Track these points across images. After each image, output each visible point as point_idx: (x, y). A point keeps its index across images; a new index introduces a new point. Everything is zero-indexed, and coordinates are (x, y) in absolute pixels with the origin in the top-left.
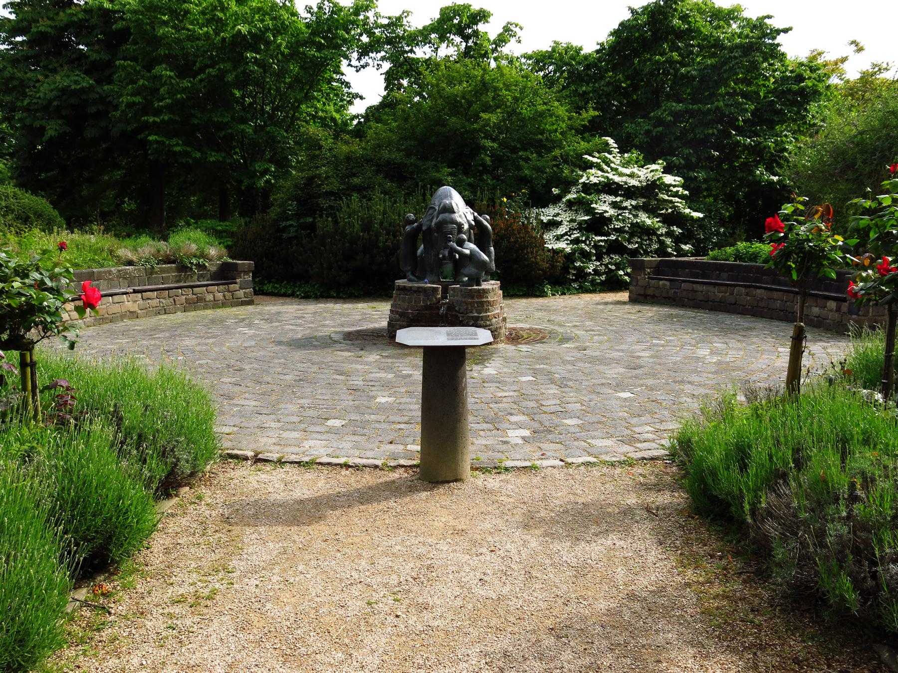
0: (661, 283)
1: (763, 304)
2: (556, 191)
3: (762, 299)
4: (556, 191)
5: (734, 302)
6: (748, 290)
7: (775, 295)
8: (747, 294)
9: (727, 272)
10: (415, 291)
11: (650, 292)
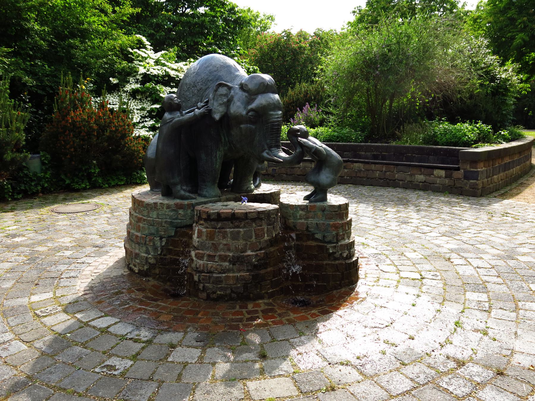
1: (362, 175)
2: (114, 81)
3: (360, 171)
4: (114, 81)
7: (373, 167)
10: (254, 220)
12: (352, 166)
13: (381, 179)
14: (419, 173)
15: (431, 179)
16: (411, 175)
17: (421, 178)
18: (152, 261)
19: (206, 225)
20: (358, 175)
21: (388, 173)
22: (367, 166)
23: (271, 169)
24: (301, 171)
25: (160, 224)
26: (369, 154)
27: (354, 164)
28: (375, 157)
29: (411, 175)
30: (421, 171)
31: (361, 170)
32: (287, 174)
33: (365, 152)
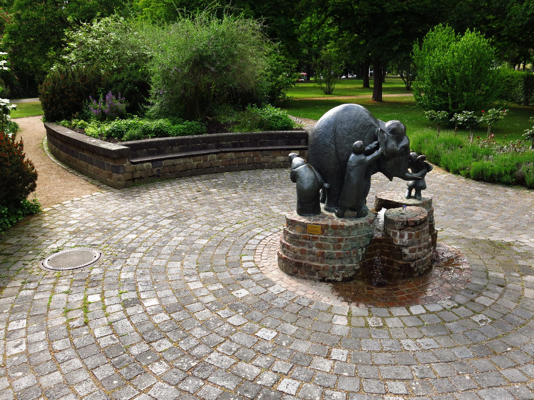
0: (145, 165)
1: (234, 162)
3: (232, 159)
5: (209, 166)
6: (219, 155)
7: (242, 154)
8: (220, 158)
9: (178, 146)
11: (137, 175)
12: (225, 156)
13: (250, 164)
16: (274, 157)
18: (357, 268)
19: (413, 229)
21: (255, 158)
22: (238, 155)
23: (155, 170)
24: (183, 167)
25: (360, 238)
27: (227, 154)
28: (235, 145)
29: (274, 157)
30: (281, 153)
32: (170, 172)
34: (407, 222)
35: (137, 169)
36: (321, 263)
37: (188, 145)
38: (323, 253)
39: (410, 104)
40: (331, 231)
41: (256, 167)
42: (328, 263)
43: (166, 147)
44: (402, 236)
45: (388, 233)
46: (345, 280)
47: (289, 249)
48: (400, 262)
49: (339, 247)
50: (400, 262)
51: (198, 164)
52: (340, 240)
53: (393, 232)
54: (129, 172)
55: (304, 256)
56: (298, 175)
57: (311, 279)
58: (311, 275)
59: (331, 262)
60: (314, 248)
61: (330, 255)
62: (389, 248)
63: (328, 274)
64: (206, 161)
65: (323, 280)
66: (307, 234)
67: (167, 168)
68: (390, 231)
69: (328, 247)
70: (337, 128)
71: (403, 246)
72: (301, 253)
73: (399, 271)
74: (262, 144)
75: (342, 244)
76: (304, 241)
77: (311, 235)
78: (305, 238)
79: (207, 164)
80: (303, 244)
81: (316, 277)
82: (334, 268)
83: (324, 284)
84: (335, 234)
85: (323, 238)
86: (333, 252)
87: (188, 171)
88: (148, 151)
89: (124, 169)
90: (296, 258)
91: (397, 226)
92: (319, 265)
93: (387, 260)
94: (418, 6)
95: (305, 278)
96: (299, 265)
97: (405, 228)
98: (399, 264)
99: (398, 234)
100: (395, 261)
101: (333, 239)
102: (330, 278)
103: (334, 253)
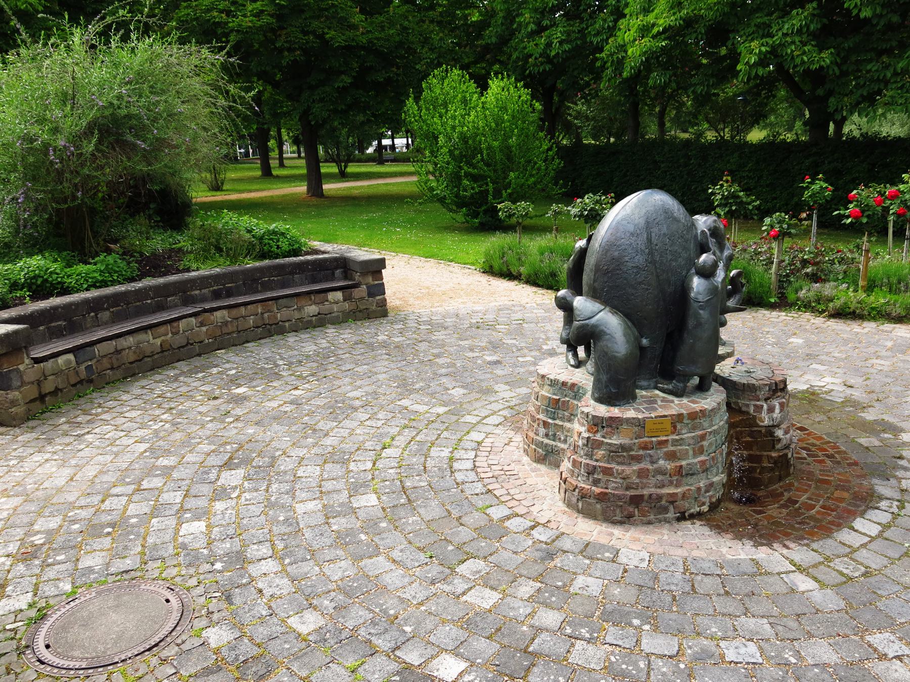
1: (231, 328)
3: (225, 323)
5: (184, 342)
8: (202, 324)
9: (107, 309)
11: (48, 387)
12: (212, 317)
14: (310, 303)
15: (326, 307)
16: (299, 309)
17: (312, 309)
20: (225, 330)
22: (235, 312)
23: (83, 367)
24: (135, 352)
26: (205, 291)
27: (215, 313)
28: (217, 295)
30: (311, 299)
31: (228, 322)
32: (112, 369)
33: (200, 290)
34: (776, 383)
35: (47, 373)
36: (677, 486)
37: (128, 305)
38: (681, 467)
39: (413, 197)
40: (688, 424)
41: (269, 331)
42: (687, 485)
43: (84, 315)
44: (771, 410)
45: (744, 409)
46: (714, 507)
47: (612, 475)
48: (774, 454)
49: (701, 451)
50: (774, 454)
51: (163, 341)
52: (703, 437)
53: (755, 405)
54: (32, 383)
55: (645, 481)
56: (602, 331)
57: (660, 521)
58: (660, 514)
59: (690, 480)
60: (661, 462)
61: (691, 469)
62: (751, 434)
63: (689, 503)
64: (177, 333)
65: (682, 517)
66: (646, 439)
67: (105, 360)
68: (748, 406)
69: (685, 455)
70: (653, 235)
71: (774, 426)
72: (639, 477)
73: (772, 470)
74: (267, 287)
75: (705, 443)
76: (641, 452)
77: (654, 439)
78: (645, 448)
79: (180, 340)
80: (638, 459)
81: (671, 515)
82: (699, 489)
83: (688, 524)
84: (694, 428)
85: (677, 440)
86: (696, 460)
87: (146, 359)
88: (48, 328)
89: (21, 377)
90: (628, 488)
91: (762, 394)
92: (675, 491)
93: (749, 455)
94: (377, 39)
95: (649, 523)
96: (636, 501)
97: (773, 395)
98: (772, 457)
99: (765, 407)
100: (765, 453)
101: (693, 438)
102: (692, 511)
103: (696, 464)
